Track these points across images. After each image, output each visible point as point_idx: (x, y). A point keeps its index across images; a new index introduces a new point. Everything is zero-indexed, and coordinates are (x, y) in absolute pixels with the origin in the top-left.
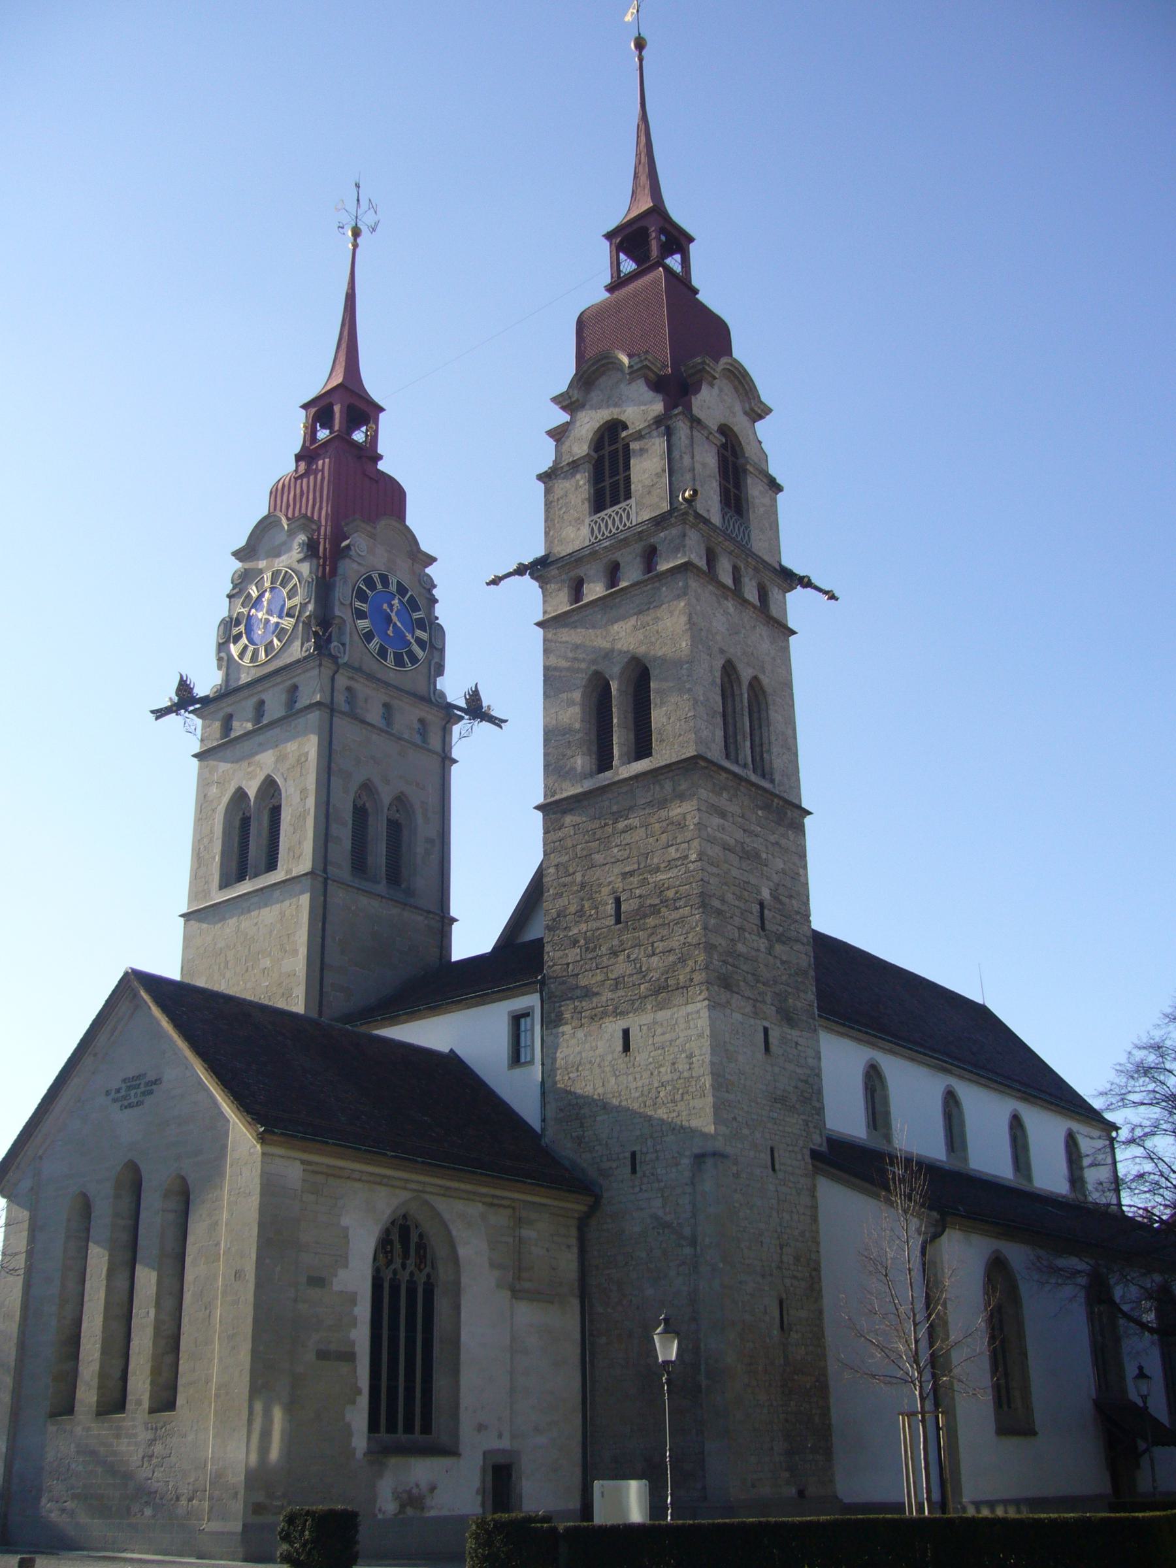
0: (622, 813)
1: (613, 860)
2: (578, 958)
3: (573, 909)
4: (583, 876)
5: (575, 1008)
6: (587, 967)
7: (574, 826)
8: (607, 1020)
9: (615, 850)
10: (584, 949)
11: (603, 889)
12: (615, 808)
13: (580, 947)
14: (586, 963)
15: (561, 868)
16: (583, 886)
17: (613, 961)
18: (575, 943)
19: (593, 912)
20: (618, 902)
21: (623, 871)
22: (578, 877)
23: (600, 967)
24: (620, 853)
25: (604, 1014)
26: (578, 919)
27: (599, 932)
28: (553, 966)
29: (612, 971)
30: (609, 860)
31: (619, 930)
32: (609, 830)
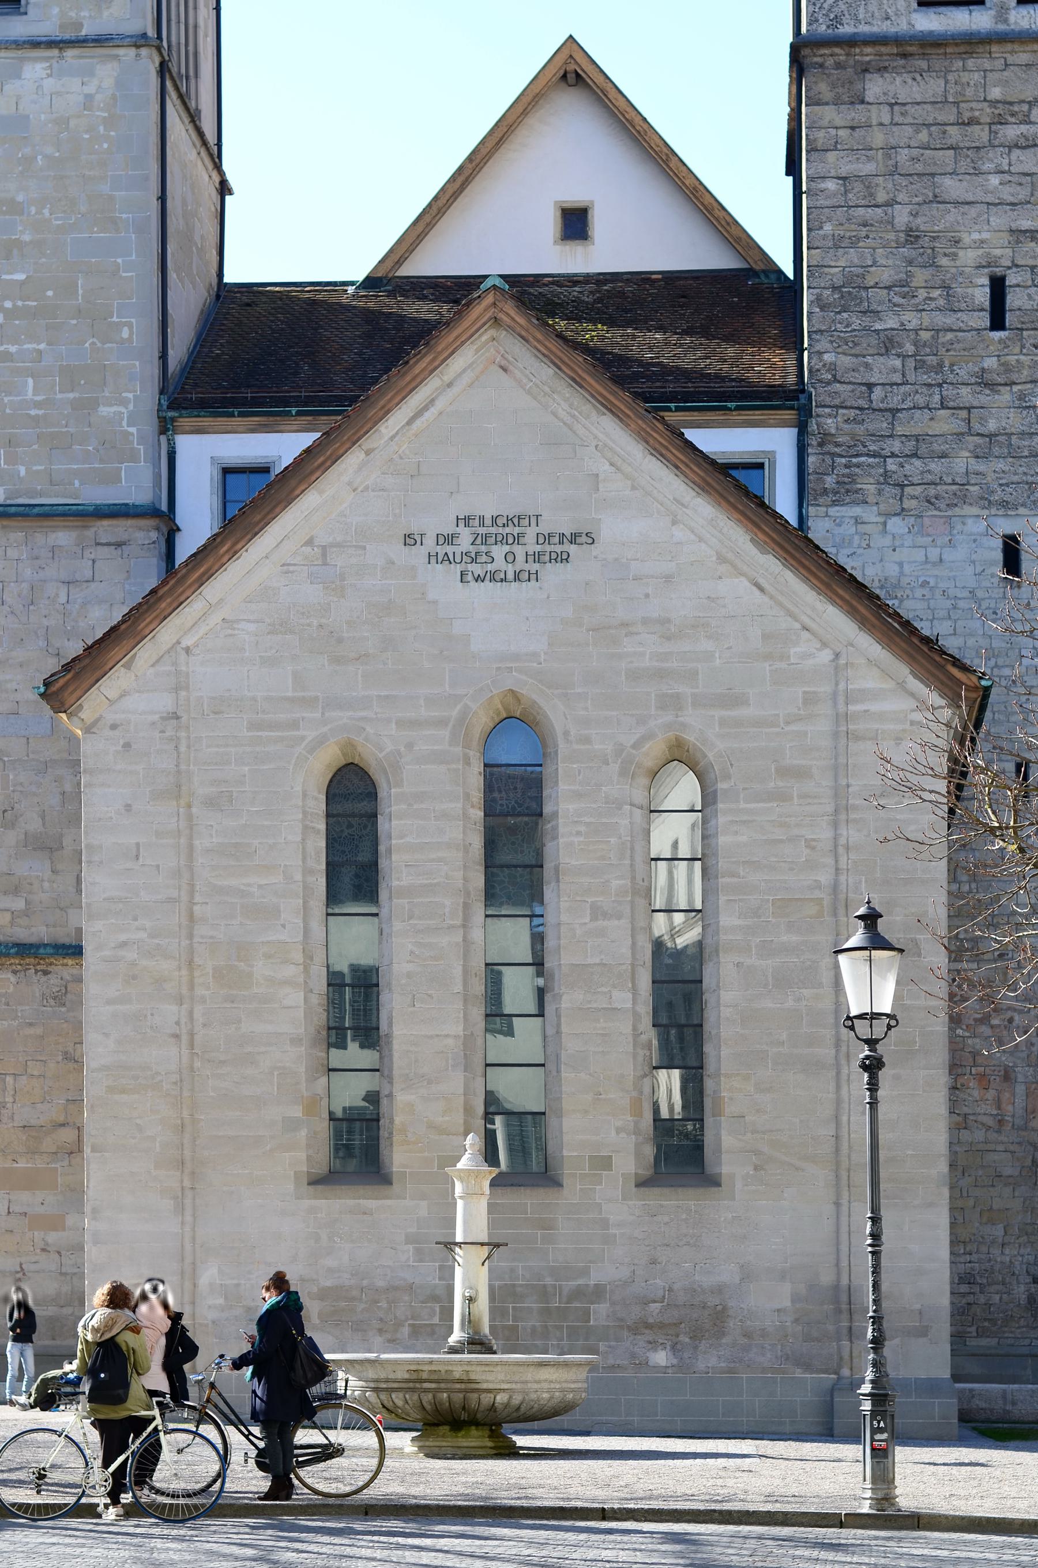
0: (1016, 108)
1: (990, 198)
2: (897, 378)
3: (886, 276)
4: (915, 215)
5: (886, 474)
6: (921, 400)
7: (891, 105)
8: (968, 510)
9: (995, 180)
10: (911, 363)
11: (961, 253)
12: (996, 93)
13: (904, 357)
14: (917, 392)
15: (858, 186)
16: (912, 236)
17: (983, 399)
18: (888, 344)
19: (936, 293)
20: (998, 287)
21: (1014, 226)
22: (902, 216)
23: (951, 404)
24: (1007, 189)
25: (964, 499)
26: (897, 299)
27: (950, 336)
28: (828, 383)
29: (983, 421)
30: (980, 196)
31: (1000, 341)
32: (980, 134)
